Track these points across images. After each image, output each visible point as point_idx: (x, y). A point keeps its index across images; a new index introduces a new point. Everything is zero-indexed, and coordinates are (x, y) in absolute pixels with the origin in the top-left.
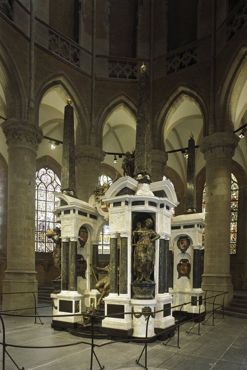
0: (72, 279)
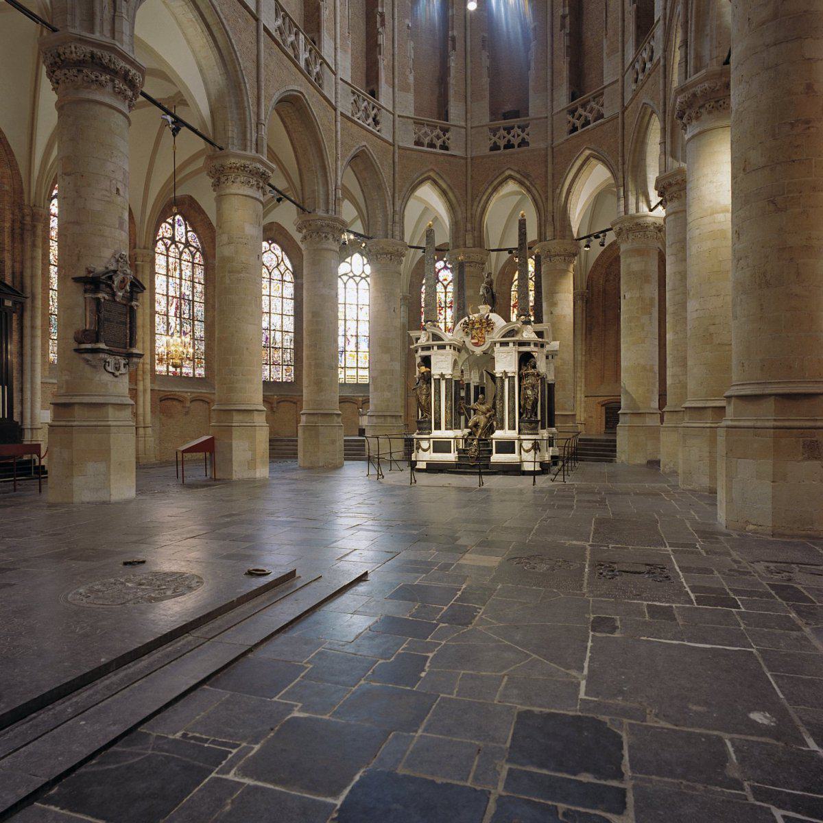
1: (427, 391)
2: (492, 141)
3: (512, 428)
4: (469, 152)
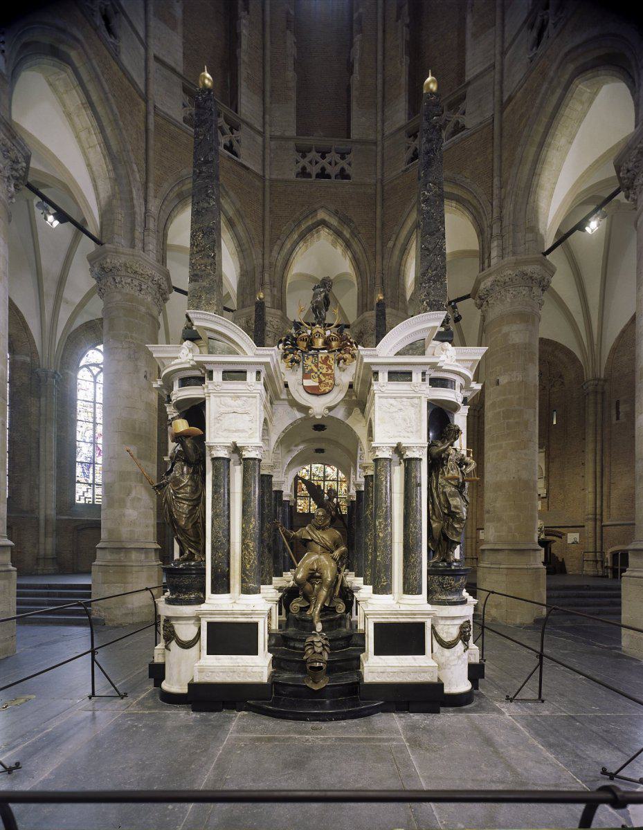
0: (254, 562)
1: (193, 492)
2: (300, 165)
3: (410, 587)
4: (267, 172)
